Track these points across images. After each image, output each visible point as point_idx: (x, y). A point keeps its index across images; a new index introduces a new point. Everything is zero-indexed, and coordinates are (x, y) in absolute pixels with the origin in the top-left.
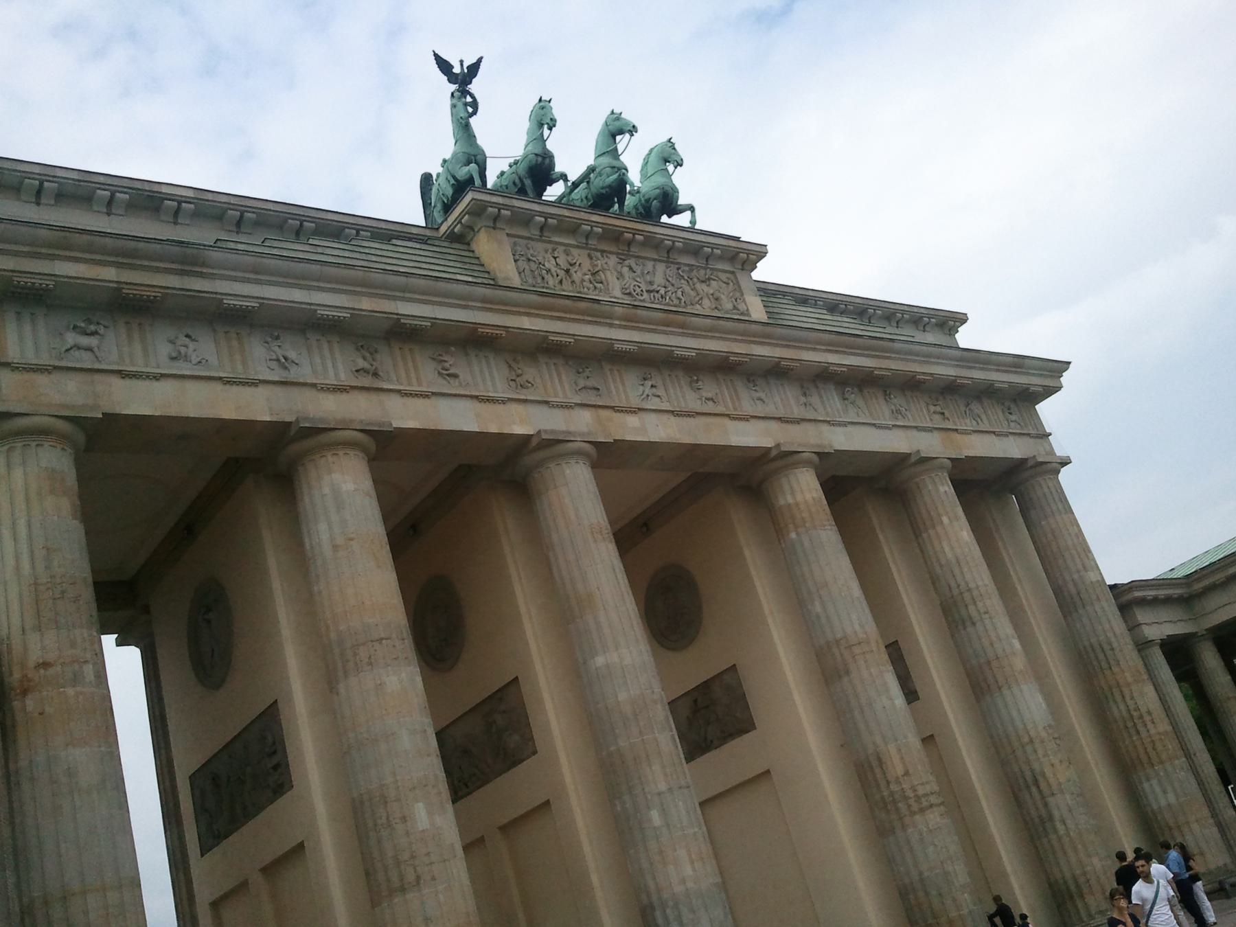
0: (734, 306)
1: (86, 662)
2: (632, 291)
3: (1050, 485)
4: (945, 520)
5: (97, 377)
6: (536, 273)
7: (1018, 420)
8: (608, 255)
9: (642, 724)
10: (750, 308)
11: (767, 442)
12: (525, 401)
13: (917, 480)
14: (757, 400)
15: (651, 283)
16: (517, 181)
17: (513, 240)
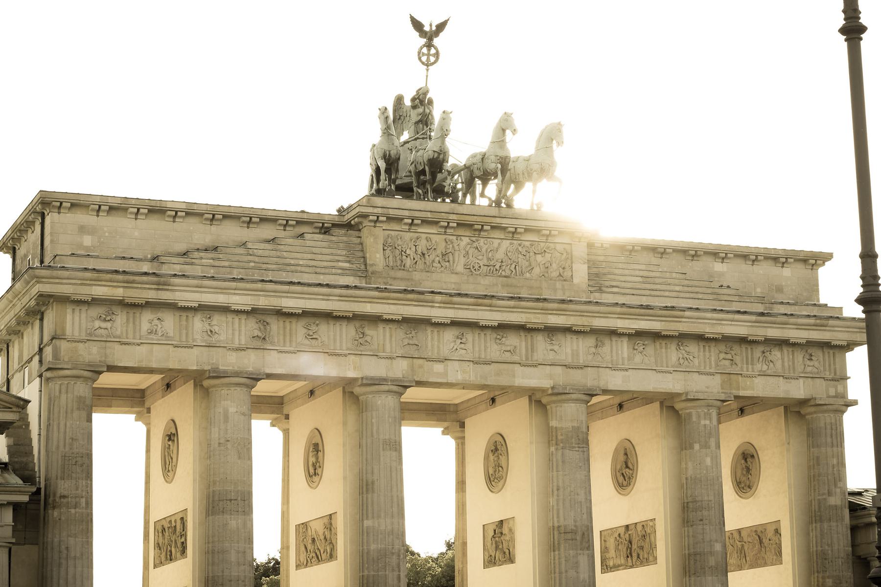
0: (560, 273)
1: (82, 497)
2: (472, 268)
3: (828, 421)
4: (697, 447)
5: (108, 344)
6: (398, 258)
7: (816, 364)
8: (463, 238)
9: (380, 565)
10: (573, 275)
11: (546, 384)
12: (361, 355)
13: (688, 411)
14: (550, 350)
15: (489, 259)
16: (422, 164)
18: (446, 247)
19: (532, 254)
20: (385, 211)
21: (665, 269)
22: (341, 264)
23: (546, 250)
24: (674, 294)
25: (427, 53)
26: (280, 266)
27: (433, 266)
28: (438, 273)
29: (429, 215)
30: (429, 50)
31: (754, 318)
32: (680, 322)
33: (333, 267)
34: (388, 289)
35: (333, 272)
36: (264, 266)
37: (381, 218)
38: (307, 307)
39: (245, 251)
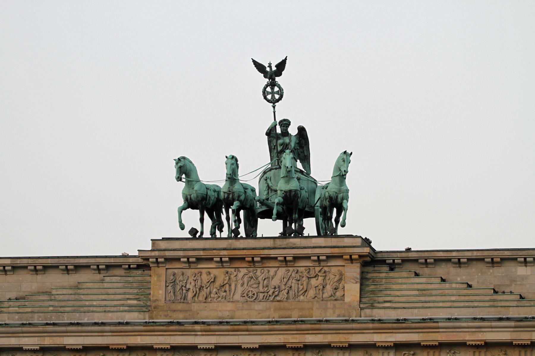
0: (332, 294)
6: (179, 292)
8: (241, 269)
17: (170, 271)
18: (224, 280)
19: (304, 279)
20: (162, 253)
21: (464, 277)
22: (129, 302)
23: (318, 274)
24: (448, 304)
25: (271, 91)
26: (75, 308)
27: (210, 297)
28: (215, 302)
29: (201, 253)
30: (272, 89)
31: (512, 324)
32: (438, 332)
33: (123, 305)
34: (155, 323)
35: (121, 309)
36: (61, 309)
37: (159, 260)
38: (84, 344)
39: (48, 297)
